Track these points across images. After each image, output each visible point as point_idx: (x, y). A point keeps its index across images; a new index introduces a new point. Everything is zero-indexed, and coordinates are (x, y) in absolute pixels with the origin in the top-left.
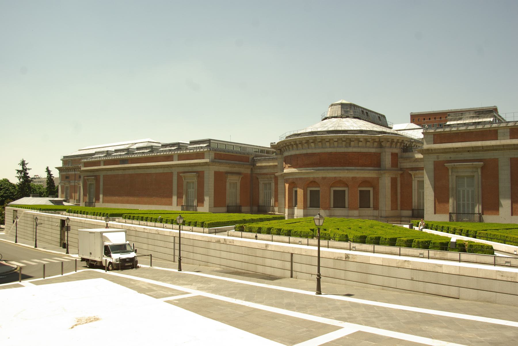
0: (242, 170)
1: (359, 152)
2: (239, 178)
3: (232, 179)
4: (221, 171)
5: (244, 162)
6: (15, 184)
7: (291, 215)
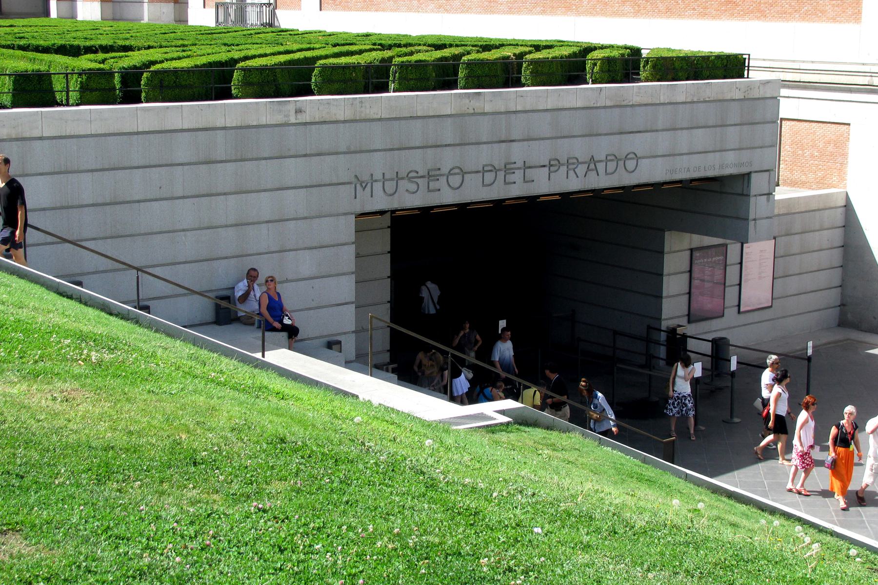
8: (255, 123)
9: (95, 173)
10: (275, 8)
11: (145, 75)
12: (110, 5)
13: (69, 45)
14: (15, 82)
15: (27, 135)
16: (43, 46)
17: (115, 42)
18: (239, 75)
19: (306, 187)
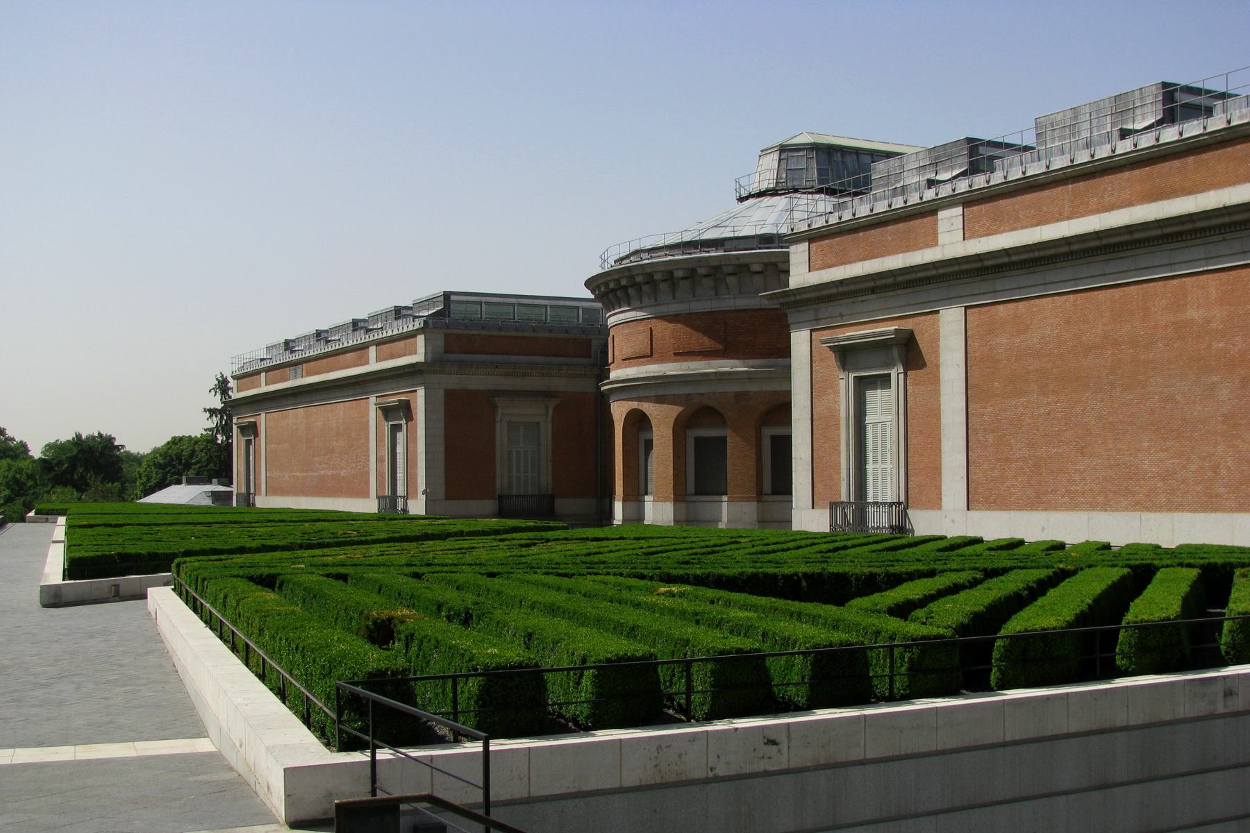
0: (560, 384)
1: (756, 307)
2: (547, 407)
3: (507, 413)
4: (470, 388)
5: (567, 357)
6: (199, 436)
7: (635, 517)
8: (1168, 717)
9: (940, 816)
10: (906, 508)
11: (999, 643)
12: (684, 505)
13: (762, 573)
14: (815, 664)
15: (842, 758)
16: (728, 576)
17: (823, 569)
18: (1131, 636)
19: (1238, 818)
